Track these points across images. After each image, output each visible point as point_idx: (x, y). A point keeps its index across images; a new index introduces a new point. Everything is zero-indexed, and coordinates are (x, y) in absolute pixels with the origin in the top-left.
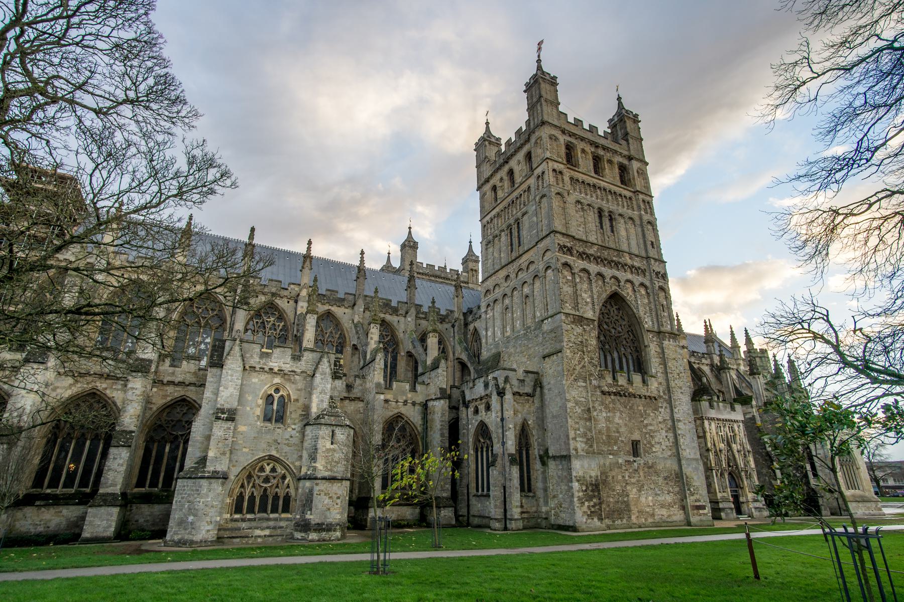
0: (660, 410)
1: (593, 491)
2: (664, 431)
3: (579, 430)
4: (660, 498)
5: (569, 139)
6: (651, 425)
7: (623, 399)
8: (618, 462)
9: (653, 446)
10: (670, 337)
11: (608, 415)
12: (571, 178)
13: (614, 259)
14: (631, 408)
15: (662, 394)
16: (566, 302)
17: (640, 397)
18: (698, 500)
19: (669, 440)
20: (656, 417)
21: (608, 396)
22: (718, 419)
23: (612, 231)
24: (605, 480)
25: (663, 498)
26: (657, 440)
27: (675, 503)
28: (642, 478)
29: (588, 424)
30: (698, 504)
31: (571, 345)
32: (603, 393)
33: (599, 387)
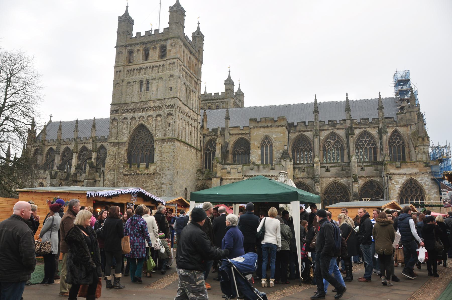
5: (130, 48)
6: (148, 187)
10: (168, 141)
11: (125, 184)
12: (128, 71)
13: (143, 106)
15: (158, 171)
17: (144, 175)
19: (157, 193)
20: (152, 183)
23: (147, 90)
32: (125, 175)
33: (123, 172)
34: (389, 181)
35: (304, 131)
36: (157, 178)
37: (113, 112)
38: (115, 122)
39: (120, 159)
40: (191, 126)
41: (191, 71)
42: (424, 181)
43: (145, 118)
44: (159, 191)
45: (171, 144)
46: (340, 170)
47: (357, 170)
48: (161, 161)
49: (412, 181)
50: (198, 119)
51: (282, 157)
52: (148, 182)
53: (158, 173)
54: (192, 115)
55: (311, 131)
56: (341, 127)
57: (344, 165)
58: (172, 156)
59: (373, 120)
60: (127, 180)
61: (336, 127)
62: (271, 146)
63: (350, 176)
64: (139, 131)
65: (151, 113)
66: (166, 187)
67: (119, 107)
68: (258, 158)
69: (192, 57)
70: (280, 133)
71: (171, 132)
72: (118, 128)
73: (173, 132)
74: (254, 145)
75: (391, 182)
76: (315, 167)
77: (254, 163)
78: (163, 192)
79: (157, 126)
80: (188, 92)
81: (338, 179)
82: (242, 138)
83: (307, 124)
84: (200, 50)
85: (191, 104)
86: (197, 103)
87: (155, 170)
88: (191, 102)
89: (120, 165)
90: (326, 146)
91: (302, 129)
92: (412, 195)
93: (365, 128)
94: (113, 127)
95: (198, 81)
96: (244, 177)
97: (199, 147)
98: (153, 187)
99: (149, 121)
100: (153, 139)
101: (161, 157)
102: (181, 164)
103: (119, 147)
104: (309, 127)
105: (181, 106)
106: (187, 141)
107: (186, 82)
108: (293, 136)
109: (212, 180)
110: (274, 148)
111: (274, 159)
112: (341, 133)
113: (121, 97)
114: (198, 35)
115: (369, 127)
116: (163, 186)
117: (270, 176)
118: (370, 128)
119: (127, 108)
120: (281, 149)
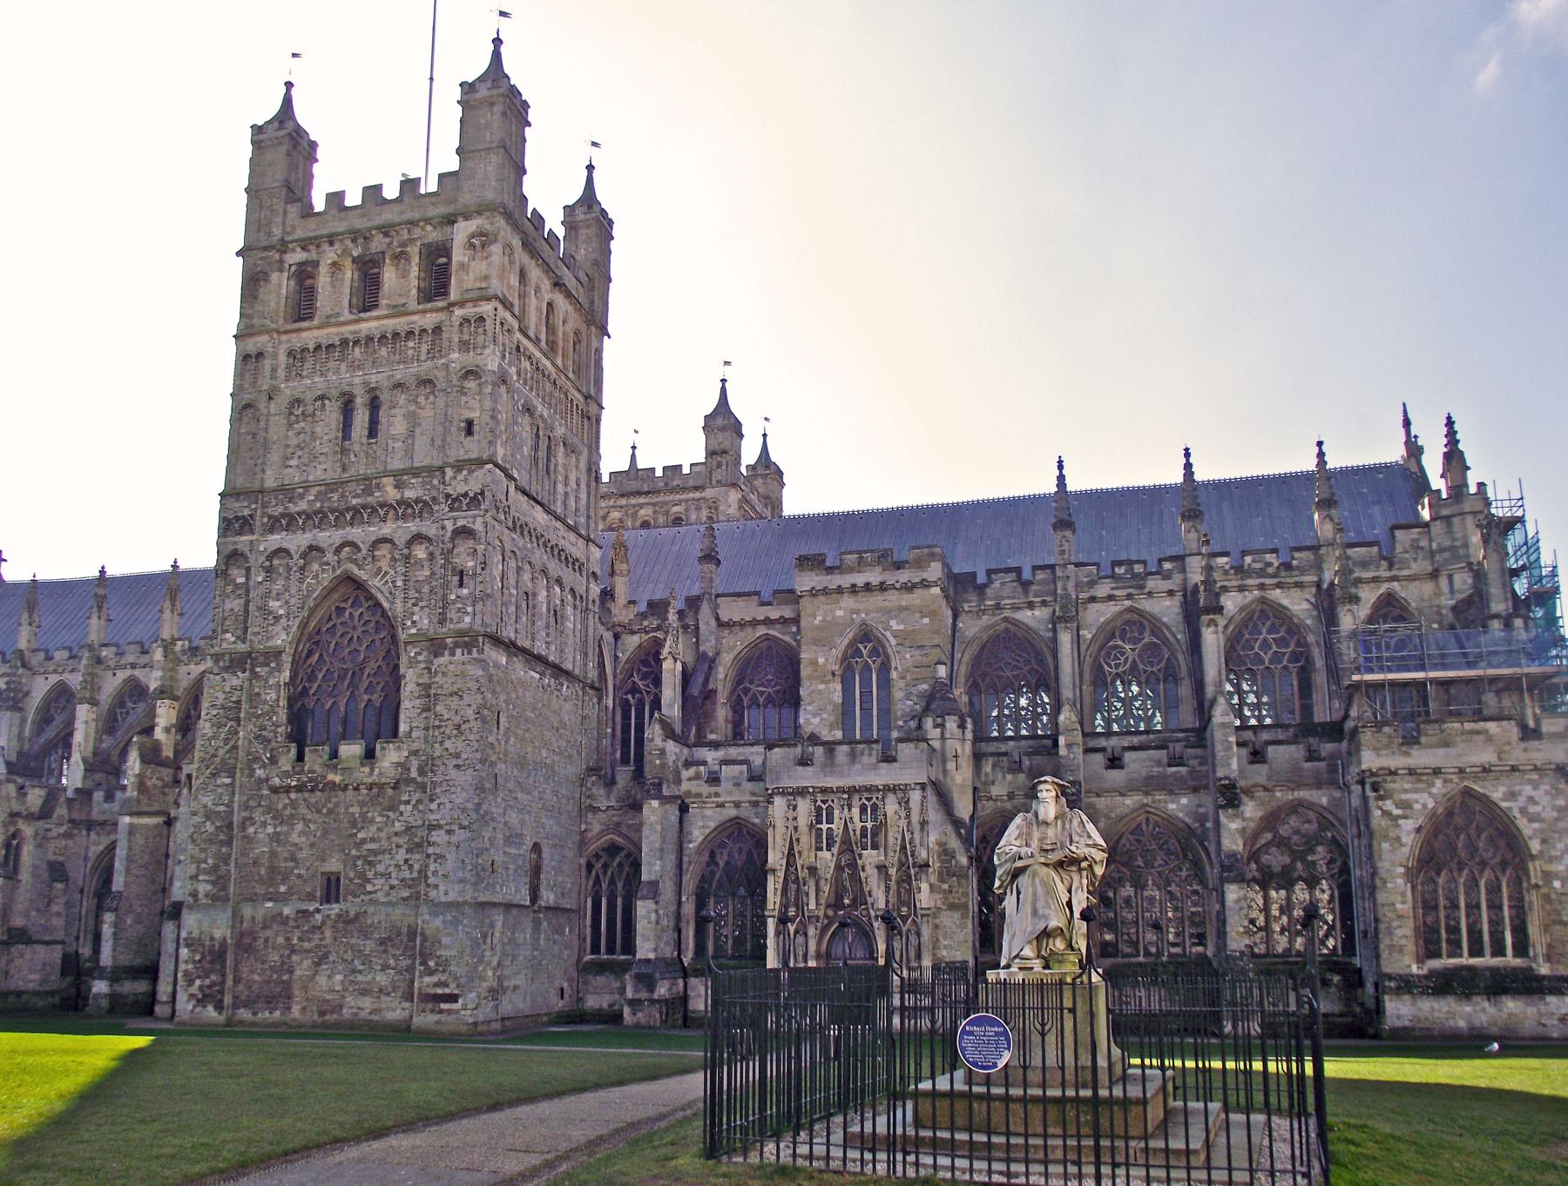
0: (402, 808)
1: (212, 962)
2: (402, 851)
3: (205, 862)
4: (360, 978)
6: (373, 840)
7: (315, 798)
8: (281, 914)
9: (369, 881)
10: (456, 645)
11: (279, 829)
14: (330, 811)
15: (414, 773)
16: (227, 631)
18: (445, 985)
19: (411, 867)
20: (389, 822)
21: (283, 795)
22: (824, 790)
24: (250, 945)
25: (369, 977)
26: (380, 868)
27: (395, 989)
28: (328, 941)
29: (224, 850)
30: (440, 991)
31: (215, 712)
33: (267, 780)
34: (1372, 803)
35: (1016, 608)
36: (408, 802)
37: (228, 525)
38: (238, 567)
39: (258, 724)
40: (557, 589)
41: (559, 362)
42: (1522, 799)
43: (364, 552)
44: (418, 856)
45: (466, 657)
46: (1165, 760)
47: (1235, 759)
48: (426, 729)
49: (1471, 802)
50: (588, 560)
51: (926, 710)
52: (372, 821)
53: (413, 780)
54: (562, 542)
55: (1044, 603)
56: (1165, 585)
57: (1178, 741)
58: (474, 707)
59: (1296, 555)
60: (287, 812)
61: (1142, 587)
62: (885, 668)
63: (1206, 787)
64: (337, 608)
65: (387, 529)
66: (446, 838)
67: (253, 506)
68: (832, 718)
69: (562, 304)
70: (918, 615)
71: (470, 609)
72: (248, 591)
73: (479, 607)
74: (814, 663)
75: (1380, 808)
76: (1063, 751)
77: (814, 739)
78: (435, 861)
79: (411, 584)
80: (543, 445)
81: (1159, 801)
82: (767, 637)
83: (1027, 575)
84: (599, 277)
85: (560, 498)
86: (583, 496)
87: (404, 766)
88: (560, 487)
89: (258, 747)
90: (1106, 668)
91: (1009, 598)
92: (1471, 863)
93: (1262, 587)
94: (230, 588)
95: (587, 405)
96: (771, 796)
97: (592, 674)
98: (395, 839)
99: (379, 564)
100: (394, 638)
101: (428, 714)
102: (512, 740)
103: (252, 670)
104: (1034, 587)
105: (511, 501)
106: (540, 648)
107: (535, 403)
108: (972, 627)
109: (645, 810)
110: (894, 675)
111: (897, 719)
112: (1166, 609)
113: (264, 463)
114: (589, 216)
115: (1279, 585)
116: (439, 836)
117: (879, 790)
118: (1282, 588)
119: (286, 508)
120: (924, 680)
